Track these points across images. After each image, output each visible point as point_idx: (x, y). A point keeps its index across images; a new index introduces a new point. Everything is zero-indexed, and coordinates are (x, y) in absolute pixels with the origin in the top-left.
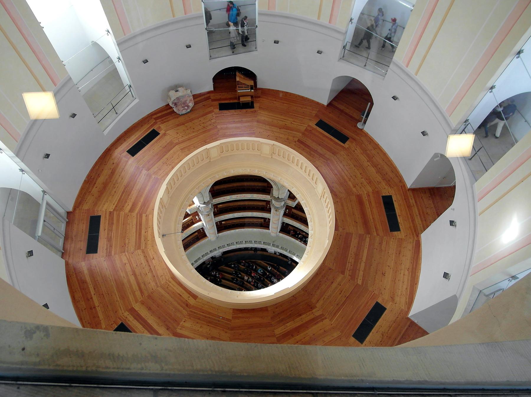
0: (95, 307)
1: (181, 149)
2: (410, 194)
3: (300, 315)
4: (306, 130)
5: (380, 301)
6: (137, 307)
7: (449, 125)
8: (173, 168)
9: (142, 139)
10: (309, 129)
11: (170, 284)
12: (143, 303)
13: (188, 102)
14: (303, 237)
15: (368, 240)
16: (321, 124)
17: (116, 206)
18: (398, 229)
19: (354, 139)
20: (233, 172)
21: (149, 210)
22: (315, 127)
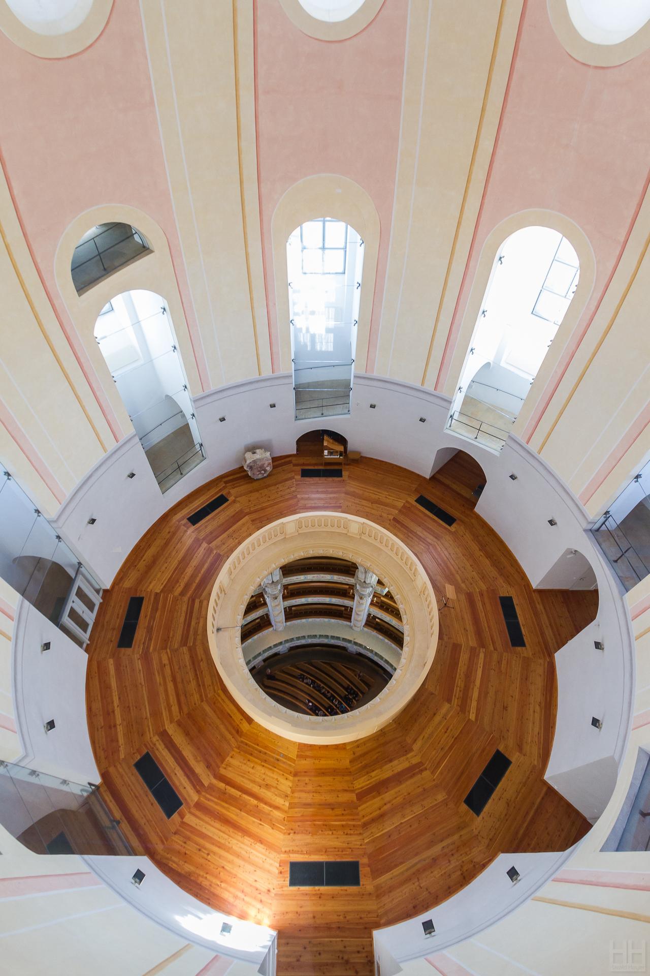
0: (115, 726)
1: (253, 521)
2: (536, 596)
3: (391, 761)
4: (404, 507)
5: (501, 749)
6: (171, 729)
9: (208, 506)
10: (408, 505)
12: (179, 724)
15: (482, 655)
16: (422, 501)
18: (522, 644)
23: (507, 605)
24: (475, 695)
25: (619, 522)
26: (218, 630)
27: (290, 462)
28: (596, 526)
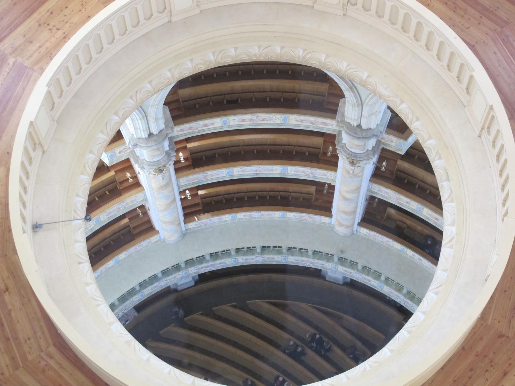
8: (66, 38)
11: (52, 363)
20: (232, 52)
26: (36, 227)
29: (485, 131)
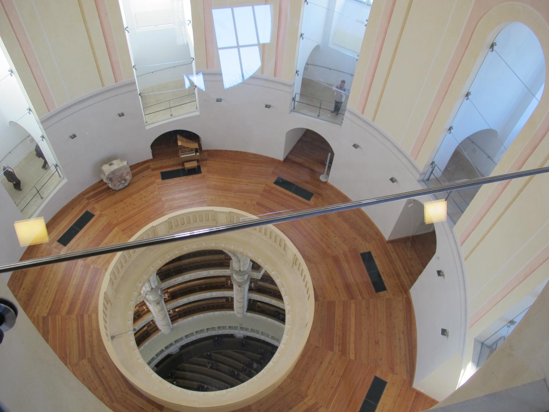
1: (123, 231)
2: (390, 247)
3: (291, 408)
4: (264, 190)
5: (378, 375)
7: (416, 169)
9: (75, 225)
11: (128, 397)
13: (124, 175)
14: (279, 315)
15: (353, 306)
16: (280, 182)
17: (50, 309)
18: (384, 289)
19: (320, 195)
20: (186, 249)
21: (91, 309)
22: (274, 186)
23: (367, 258)
24: (352, 338)
25: (443, 169)
27: (148, 168)
28: (426, 177)
29: (294, 265)
